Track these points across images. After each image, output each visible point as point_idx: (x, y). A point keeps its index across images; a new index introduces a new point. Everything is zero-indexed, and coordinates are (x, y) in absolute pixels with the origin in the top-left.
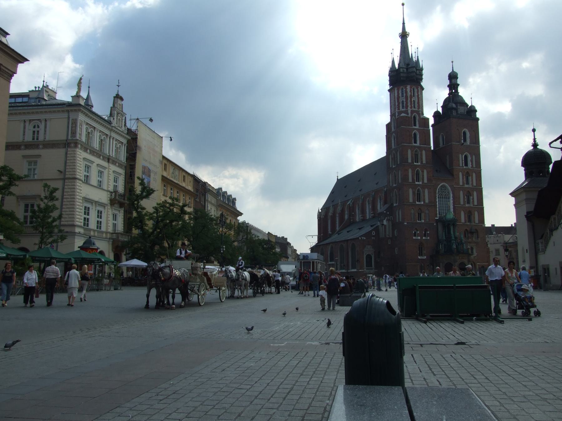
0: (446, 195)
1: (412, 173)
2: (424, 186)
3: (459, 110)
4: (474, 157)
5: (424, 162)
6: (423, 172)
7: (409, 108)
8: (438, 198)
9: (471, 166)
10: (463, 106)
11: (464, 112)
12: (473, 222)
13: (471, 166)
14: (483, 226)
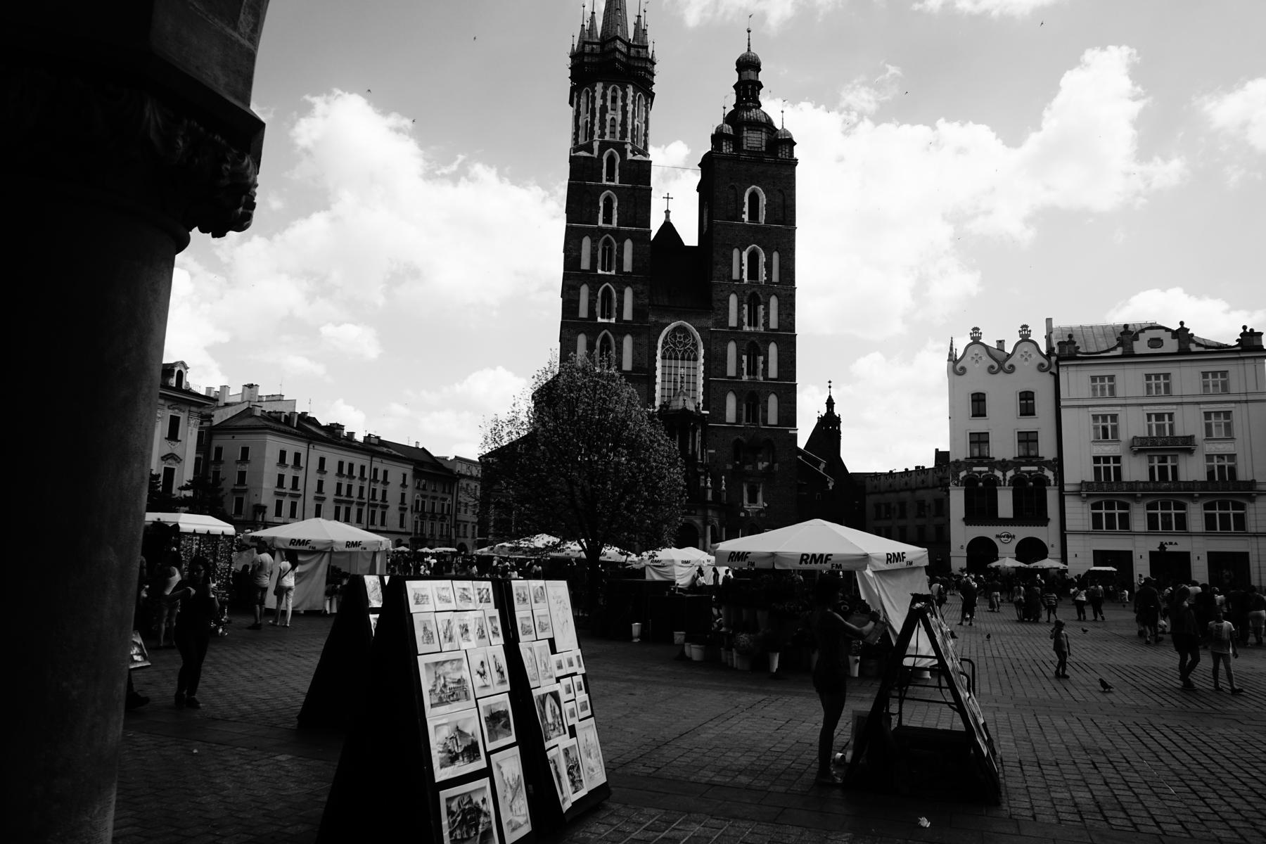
0: (685, 351)
1: (590, 295)
2: (621, 329)
3: (745, 141)
4: (776, 256)
5: (628, 267)
6: (621, 293)
7: (596, 137)
8: (663, 358)
9: (766, 278)
10: (758, 130)
11: (760, 146)
12: (761, 423)
13: (766, 278)
14: (790, 432)
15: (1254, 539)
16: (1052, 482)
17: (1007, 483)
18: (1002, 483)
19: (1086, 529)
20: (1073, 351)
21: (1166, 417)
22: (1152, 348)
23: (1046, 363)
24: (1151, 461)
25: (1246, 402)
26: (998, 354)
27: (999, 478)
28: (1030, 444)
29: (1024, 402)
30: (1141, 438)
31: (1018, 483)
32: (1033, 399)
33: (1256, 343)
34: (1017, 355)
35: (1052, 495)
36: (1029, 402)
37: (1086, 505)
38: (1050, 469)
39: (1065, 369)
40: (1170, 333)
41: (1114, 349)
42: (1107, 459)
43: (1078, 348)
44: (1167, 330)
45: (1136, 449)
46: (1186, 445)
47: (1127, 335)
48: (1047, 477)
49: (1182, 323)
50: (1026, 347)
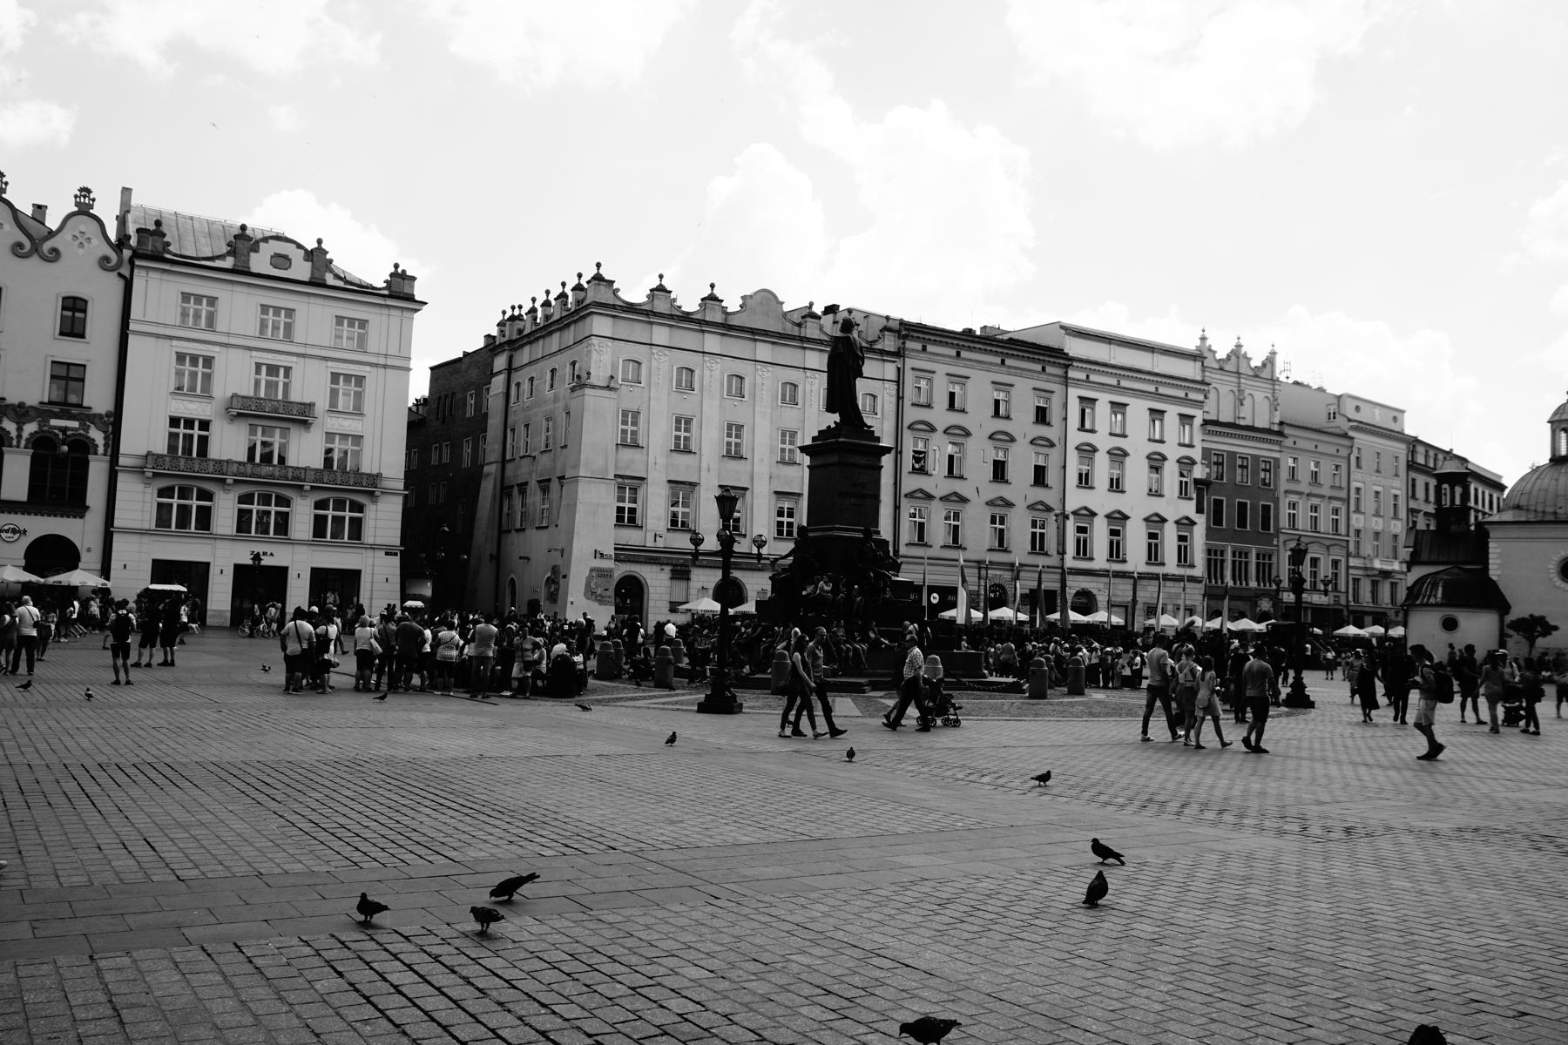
15: (370, 553)
16: (101, 450)
17: (23, 443)
18: (14, 443)
19: (146, 526)
20: (160, 248)
21: (282, 372)
22: (274, 267)
23: (114, 257)
24: (253, 431)
25: (385, 366)
26: (33, 227)
27: (9, 433)
28: (72, 384)
29: (69, 314)
30: (243, 397)
31: (42, 446)
32: (84, 311)
33: (407, 290)
34: (67, 235)
35: (97, 470)
36: (78, 315)
37: (149, 490)
38: (98, 428)
39: (143, 273)
40: (303, 251)
41: (221, 257)
42: (189, 423)
43: (168, 244)
44: (299, 246)
45: (234, 412)
46: (302, 417)
47: (243, 242)
48: (94, 440)
49: (320, 241)
50: (83, 224)
